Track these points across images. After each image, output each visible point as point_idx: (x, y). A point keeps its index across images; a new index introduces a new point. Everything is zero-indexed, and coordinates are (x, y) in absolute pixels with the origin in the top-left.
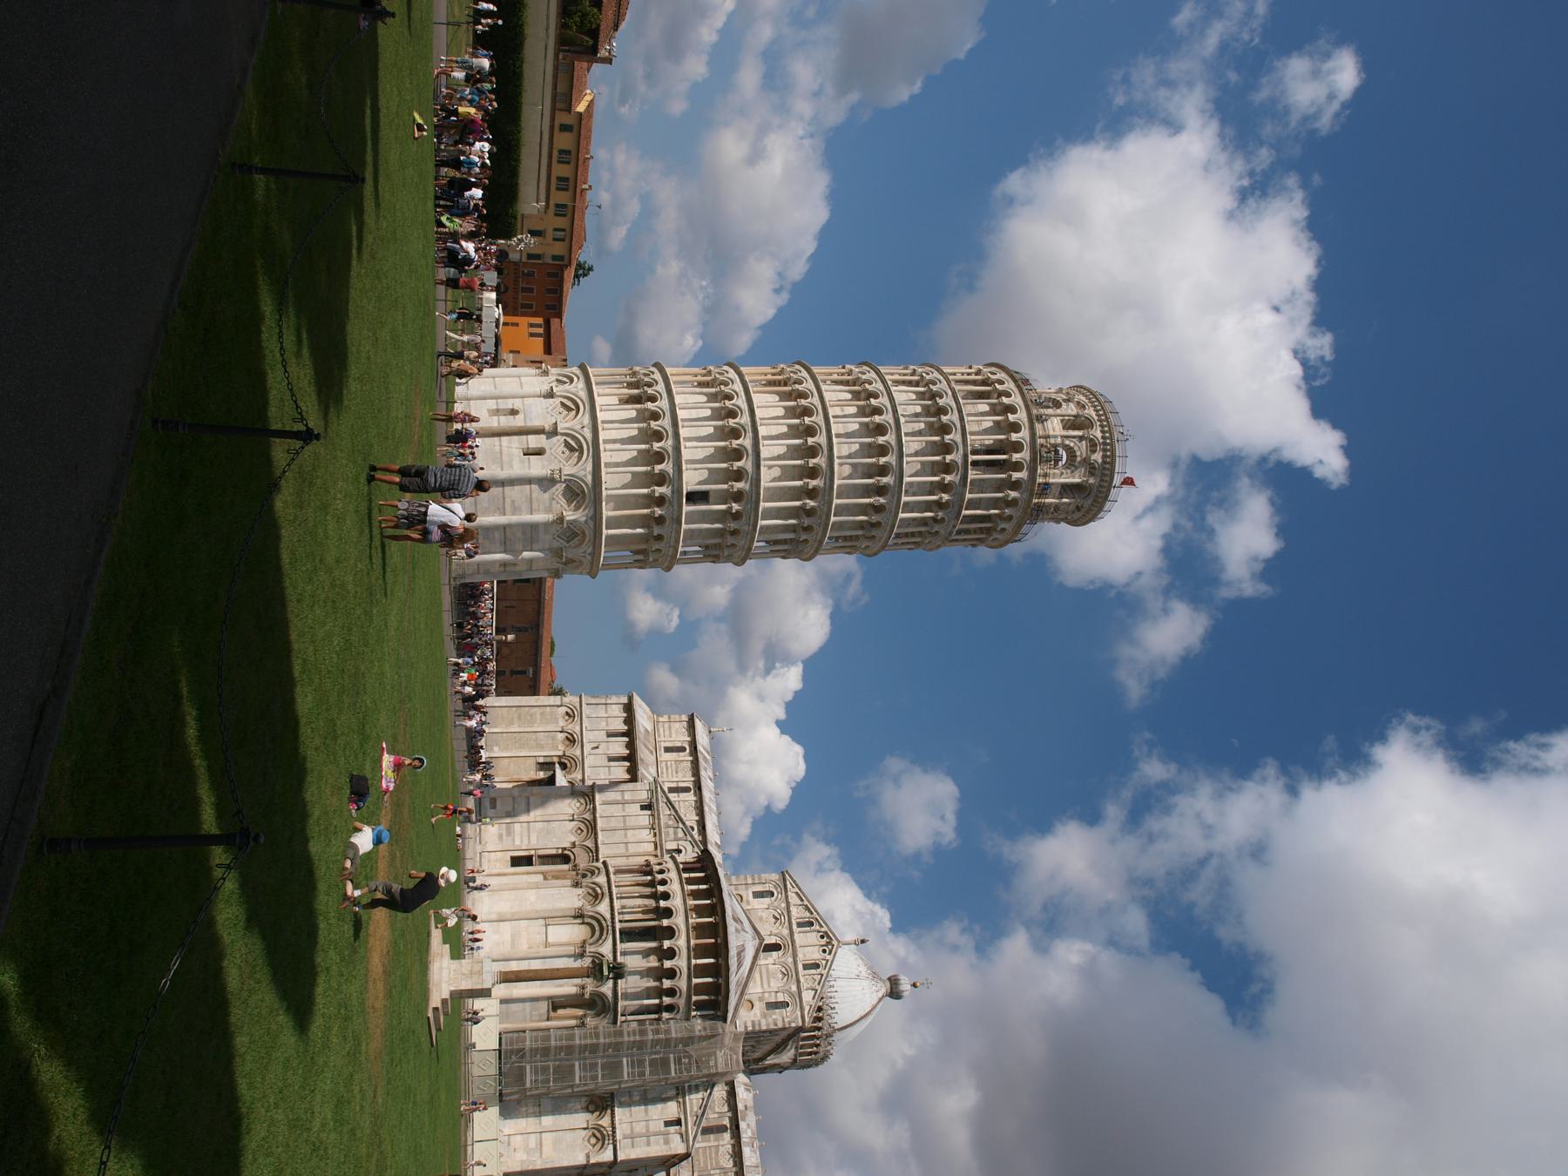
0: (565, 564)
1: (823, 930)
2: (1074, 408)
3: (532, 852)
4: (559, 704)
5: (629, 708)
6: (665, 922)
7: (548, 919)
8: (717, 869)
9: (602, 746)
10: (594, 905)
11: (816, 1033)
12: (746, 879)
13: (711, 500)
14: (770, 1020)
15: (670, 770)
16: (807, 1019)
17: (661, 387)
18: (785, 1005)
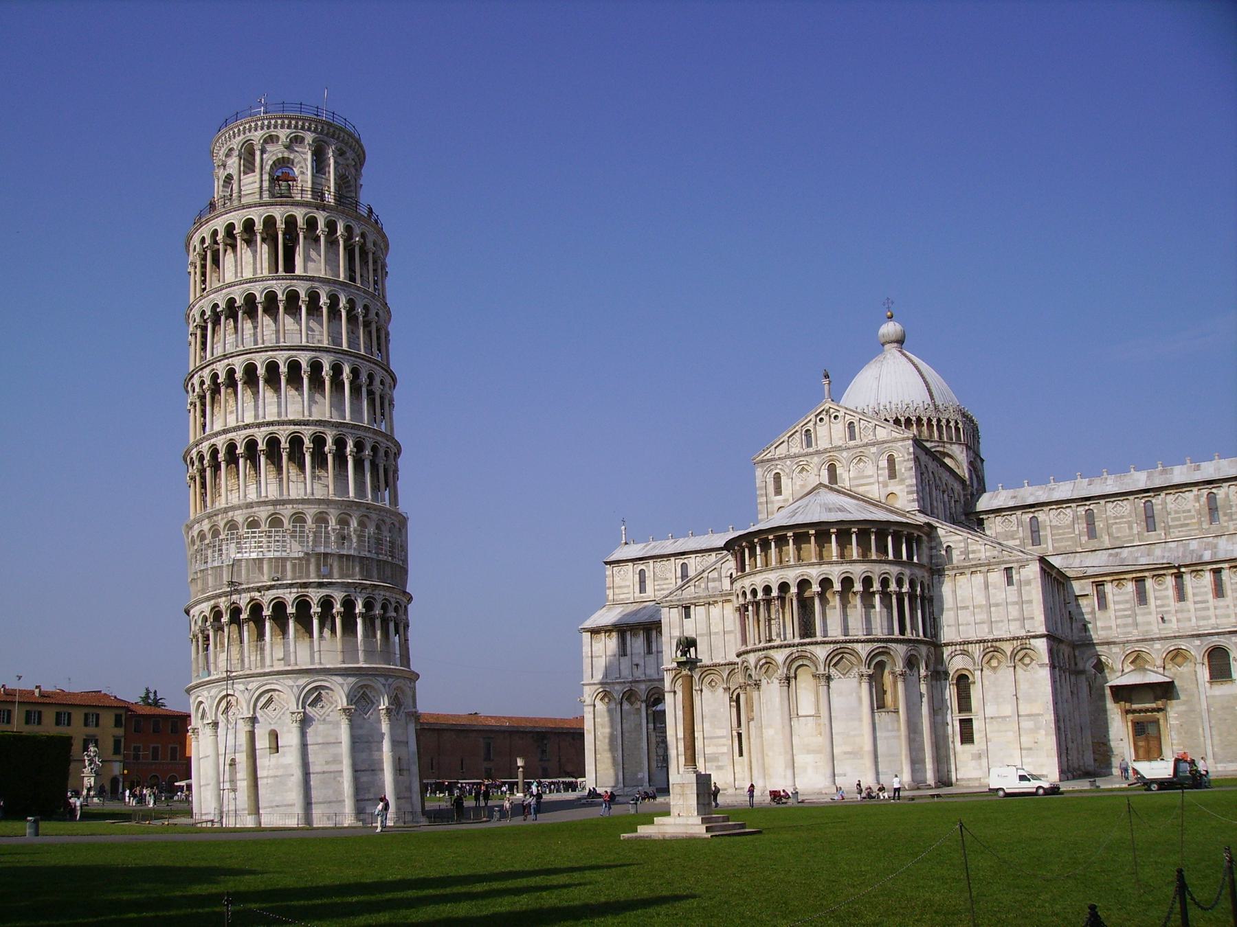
1: (814, 419)
4: (592, 708)
5: (595, 631)
7: (792, 714)
9: (636, 660)
12: (761, 503)
14: (906, 475)
15: (664, 586)
18: (891, 460)
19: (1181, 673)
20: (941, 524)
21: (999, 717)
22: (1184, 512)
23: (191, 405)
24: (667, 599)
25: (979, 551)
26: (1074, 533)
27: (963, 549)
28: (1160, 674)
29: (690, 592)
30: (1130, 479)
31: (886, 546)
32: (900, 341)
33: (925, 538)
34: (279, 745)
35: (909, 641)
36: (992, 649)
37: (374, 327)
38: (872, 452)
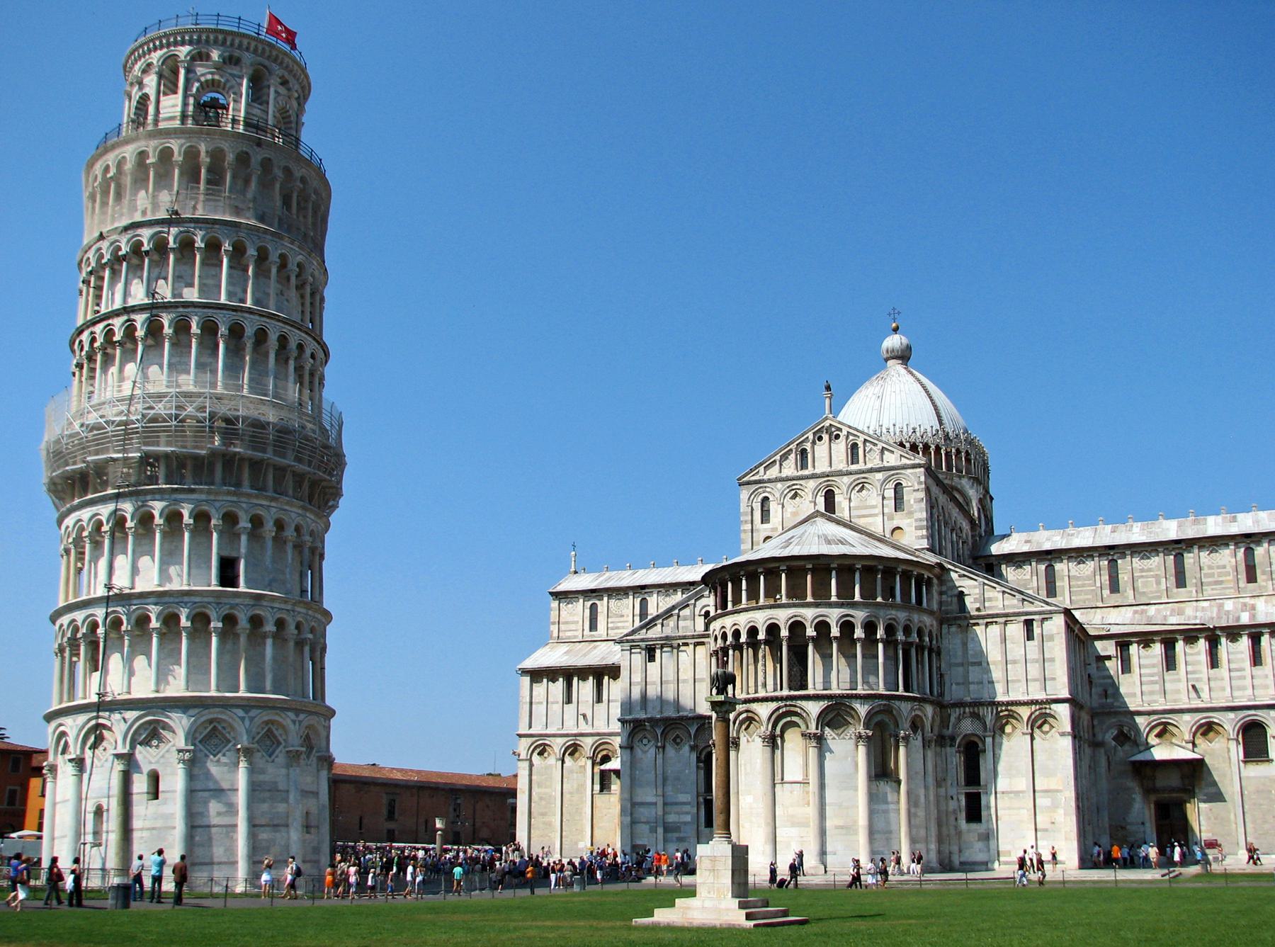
0: (310, 748)
1: (811, 437)
2: (150, 78)
3: (701, 799)
5: (537, 675)
6: (784, 633)
7: (775, 779)
8: (724, 567)
10: (760, 723)
11: (943, 452)
12: (745, 531)
13: (234, 554)
15: (619, 625)
16: (917, 461)
17: (79, 616)
18: (898, 488)
19: (1212, 749)
20: (954, 565)
21: (1011, 792)
22: (1218, 567)
23: (76, 366)
24: (628, 638)
25: (997, 599)
26: (1095, 585)
27: (977, 596)
28: (1188, 749)
29: (656, 632)
30: (1159, 528)
31: (893, 589)
32: (904, 356)
33: (935, 581)
34: (161, 788)
35: (914, 699)
36: (1006, 713)
37: (308, 290)
38: (877, 478)
